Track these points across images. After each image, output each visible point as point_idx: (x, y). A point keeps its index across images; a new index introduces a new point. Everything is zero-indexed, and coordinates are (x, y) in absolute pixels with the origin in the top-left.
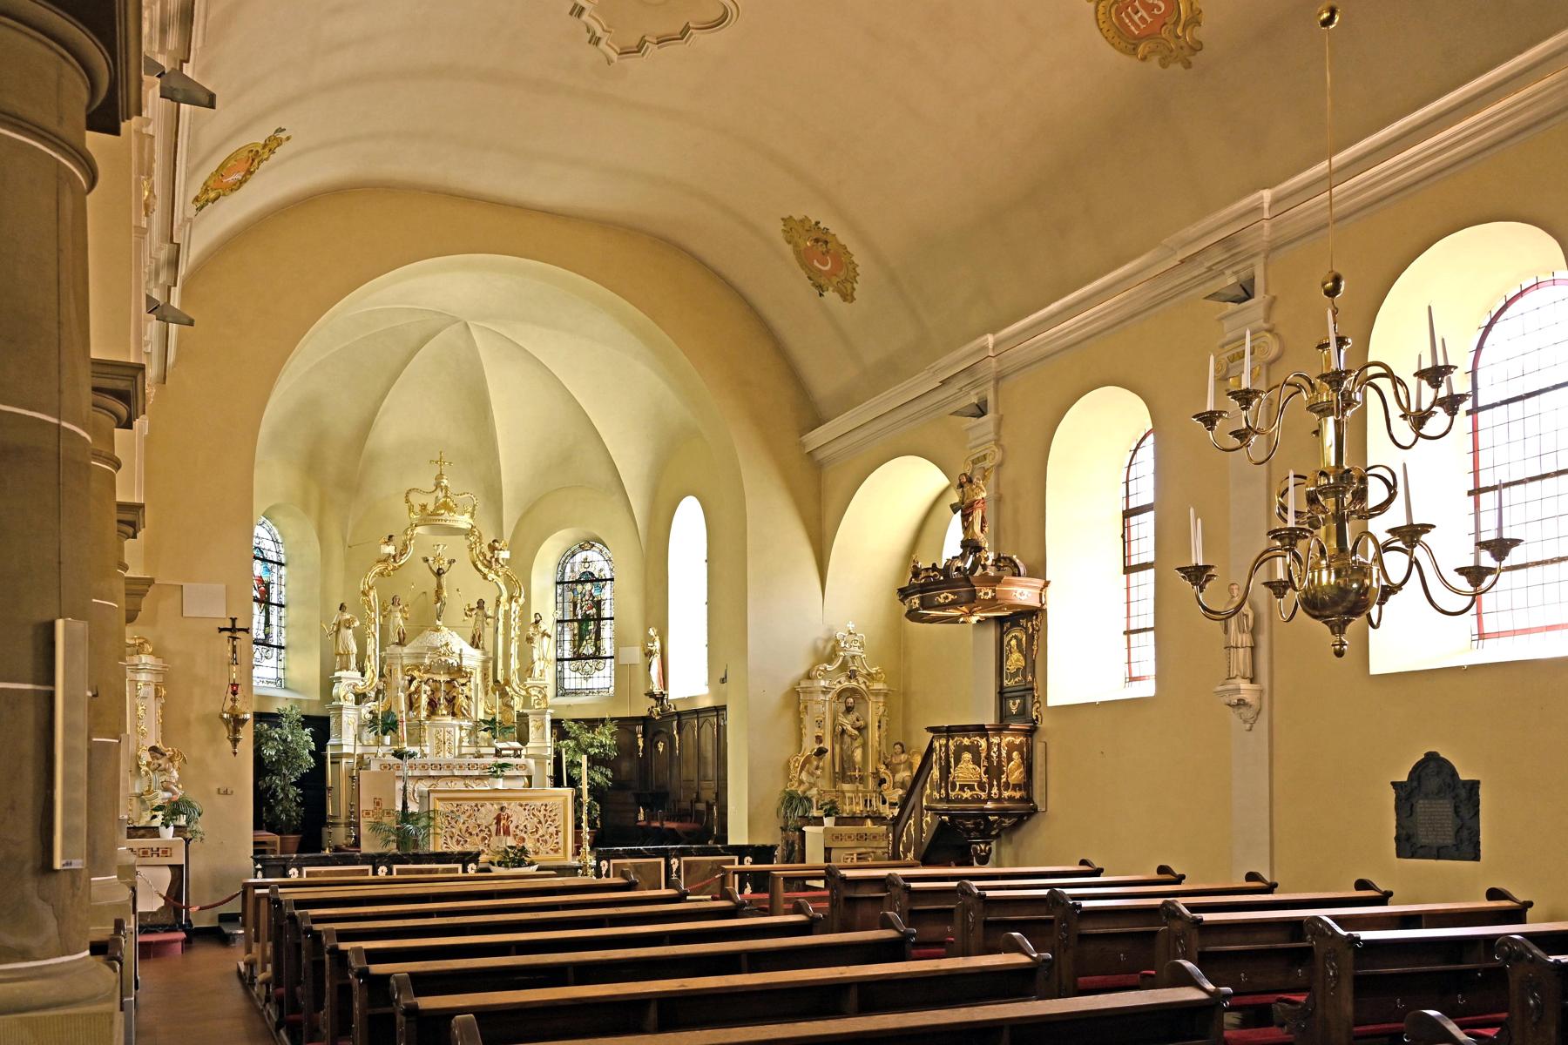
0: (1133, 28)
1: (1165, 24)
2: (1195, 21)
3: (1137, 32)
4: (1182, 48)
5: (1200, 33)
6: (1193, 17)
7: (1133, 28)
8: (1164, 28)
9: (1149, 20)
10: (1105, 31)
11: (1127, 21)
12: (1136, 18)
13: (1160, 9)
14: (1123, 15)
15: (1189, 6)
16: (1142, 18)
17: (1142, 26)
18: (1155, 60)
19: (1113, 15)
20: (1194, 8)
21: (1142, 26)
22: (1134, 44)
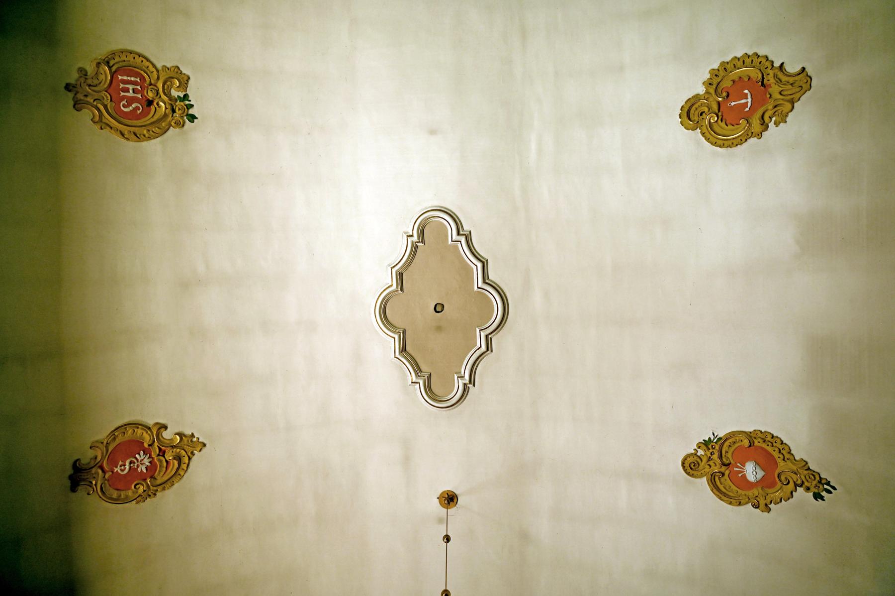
0: (125, 78)
1: (111, 101)
2: (100, 122)
3: (120, 77)
4: (86, 96)
5: (86, 115)
6: (101, 121)
7: (125, 78)
8: (109, 98)
9: (122, 94)
10: (137, 57)
11: (133, 79)
12: (131, 87)
13: (124, 106)
14: (139, 88)
15: (112, 125)
16: (127, 90)
17: (122, 86)
18: (90, 69)
19: (142, 72)
20: (108, 128)
21: (122, 86)
22: (112, 66)
